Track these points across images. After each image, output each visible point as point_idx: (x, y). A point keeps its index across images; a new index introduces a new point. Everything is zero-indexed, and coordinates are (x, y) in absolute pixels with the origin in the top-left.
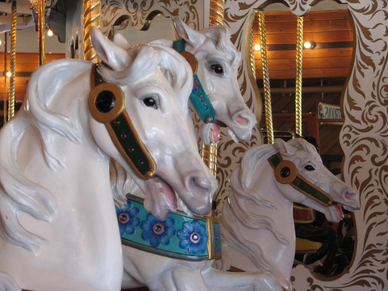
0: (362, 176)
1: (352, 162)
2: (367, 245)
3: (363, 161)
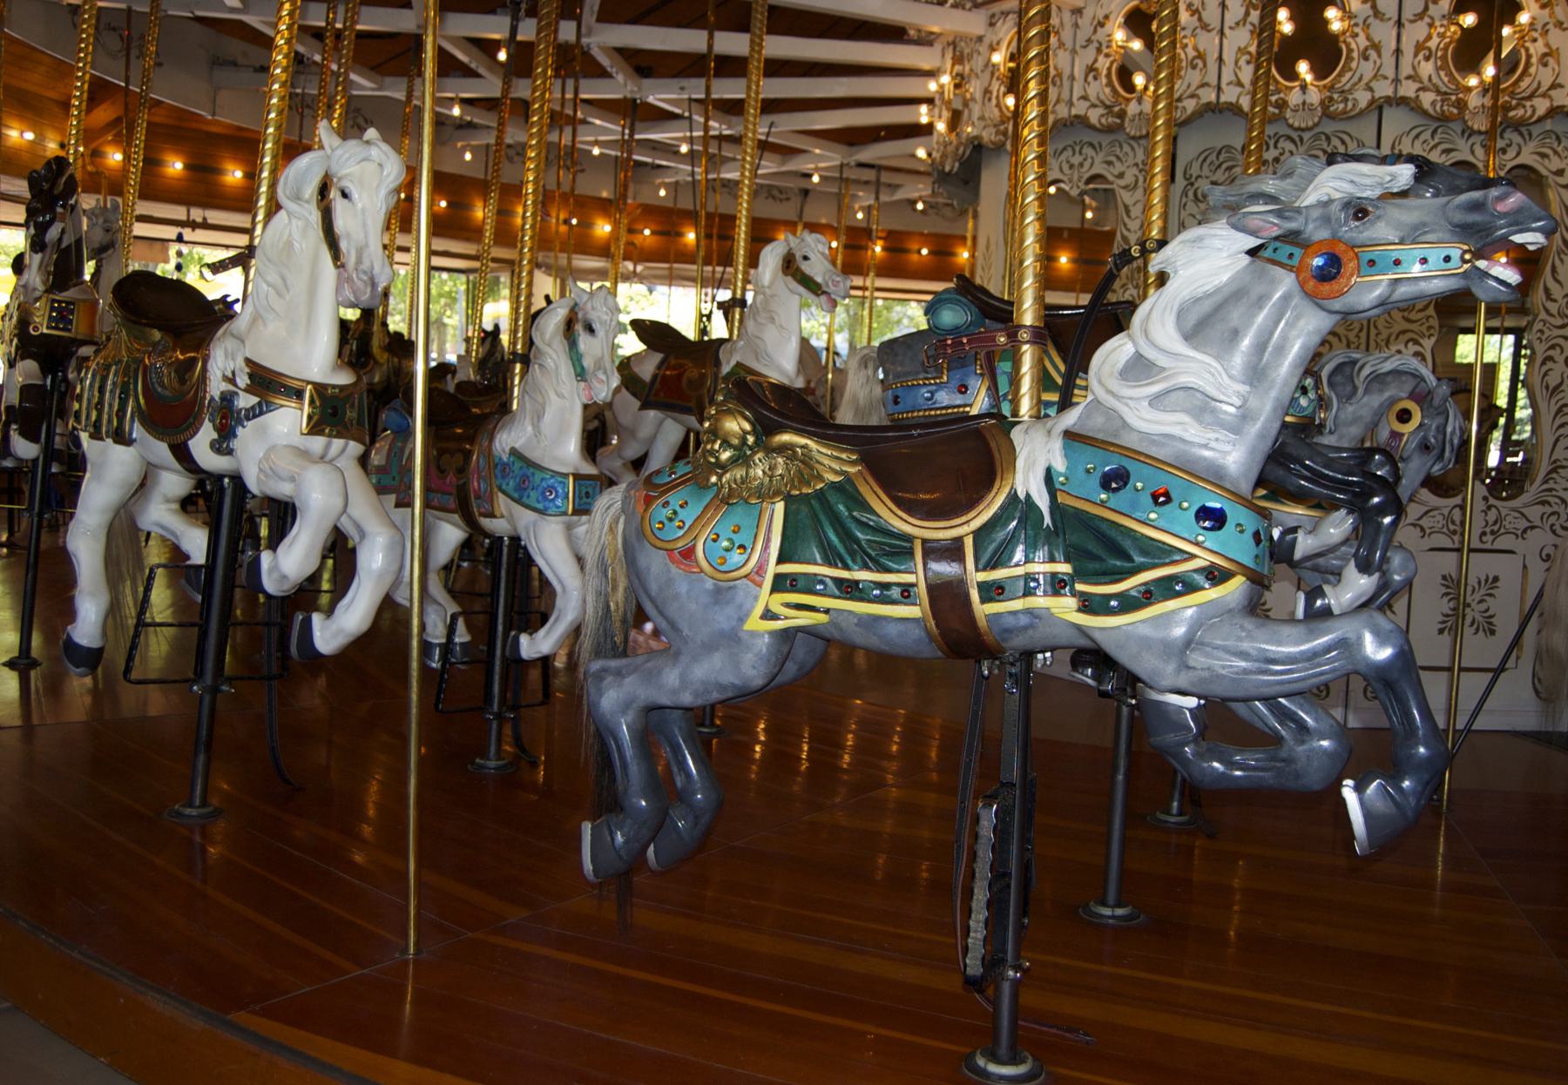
1: (1543, 363)
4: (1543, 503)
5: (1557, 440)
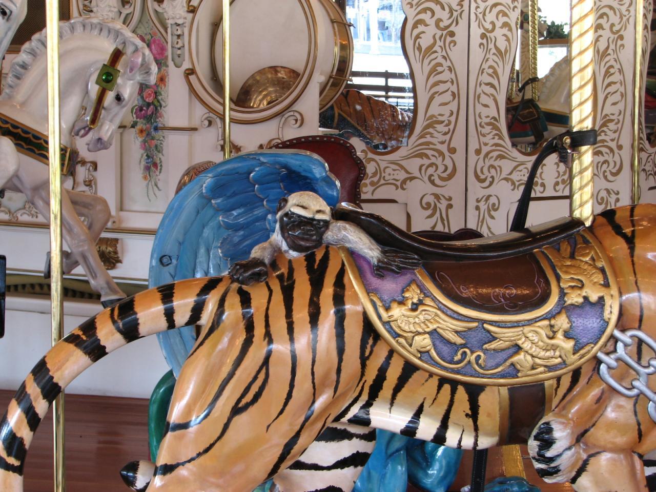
0: (425, 42)
1: (415, 26)
2: (427, 116)
3: (426, 25)
4: (422, 156)
5: (432, 98)
